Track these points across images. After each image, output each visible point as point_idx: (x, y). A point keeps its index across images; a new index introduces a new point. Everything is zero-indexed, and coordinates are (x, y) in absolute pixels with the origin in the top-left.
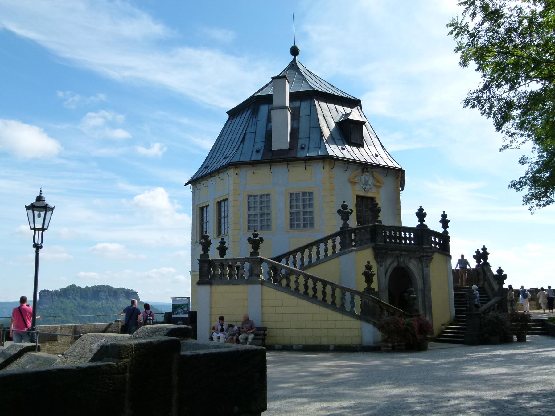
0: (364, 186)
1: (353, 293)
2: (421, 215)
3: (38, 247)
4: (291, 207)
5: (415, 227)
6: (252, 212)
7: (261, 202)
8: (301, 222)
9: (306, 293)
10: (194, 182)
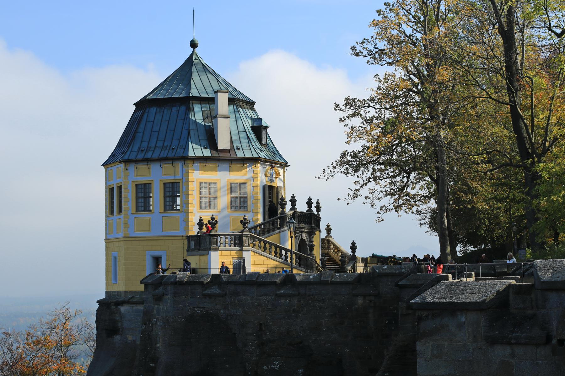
5: (305, 211)
6: (203, 195)
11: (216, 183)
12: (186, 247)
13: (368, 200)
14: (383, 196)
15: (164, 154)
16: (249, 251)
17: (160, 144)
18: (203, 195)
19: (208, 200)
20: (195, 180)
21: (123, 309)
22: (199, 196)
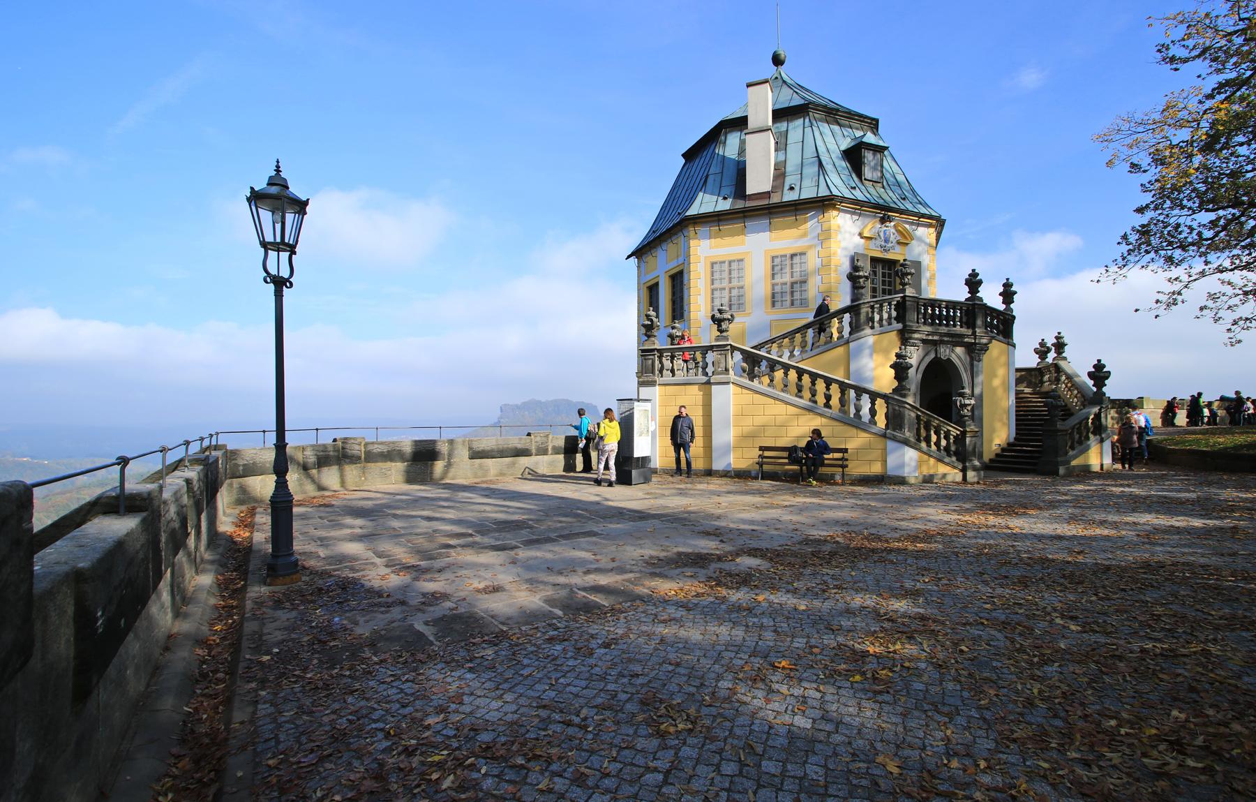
0: (883, 243)
1: (874, 396)
2: (973, 283)
3: (280, 284)
5: (963, 300)
6: (717, 285)
7: (730, 271)
10: (640, 253)
11: (742, 260)
13: (1205, 312)
14: (1239, 303)
16: (727, 383)
18: (717, 285)
19: (726, 293)
20: (702, 260)
22: (709, 287)
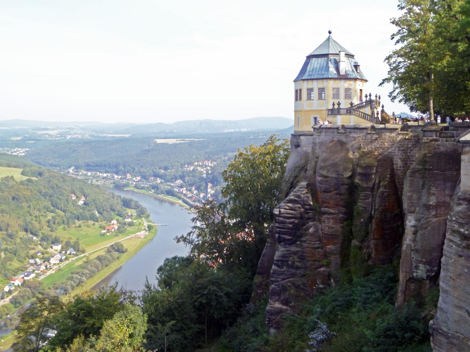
4: (345, 92)
8: (348, 97)
9: (363, 117)
12: (327, 114)
15: (318, 77)
17: (317, 73)
21: (302, 138)
